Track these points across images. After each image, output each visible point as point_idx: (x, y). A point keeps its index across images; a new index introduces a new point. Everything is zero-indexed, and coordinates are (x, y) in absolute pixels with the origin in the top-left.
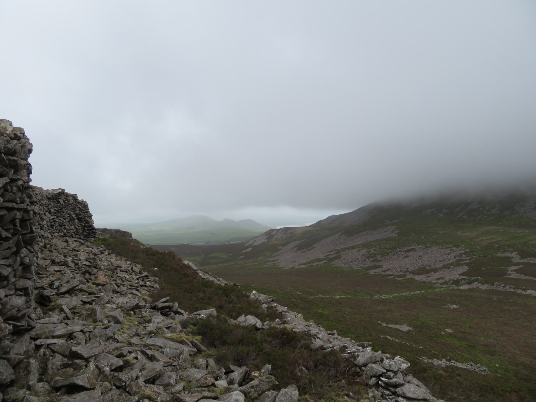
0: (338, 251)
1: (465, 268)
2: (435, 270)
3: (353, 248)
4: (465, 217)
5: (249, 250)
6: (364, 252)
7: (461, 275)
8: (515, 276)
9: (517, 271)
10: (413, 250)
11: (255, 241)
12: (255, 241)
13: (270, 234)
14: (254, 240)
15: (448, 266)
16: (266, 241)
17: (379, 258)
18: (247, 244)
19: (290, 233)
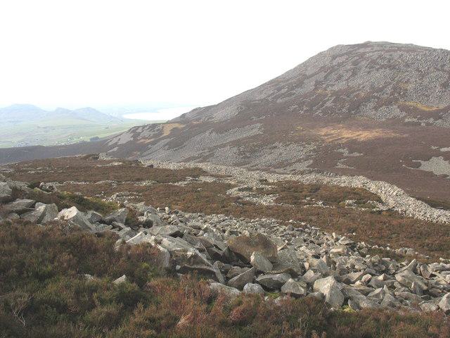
0: (211, 150)
1: (312, 161)
2: (290, 164)
3: (224, 146)
4: (321, 115)
5: (115, 149)
6: (235, 149)
7: (308, 167)
8: (340, 166)
9: (343, 163)
10: (275, 147)
11: (119, 139)
12: (119, 139)
13: (135, 131)
14: (119, 137)
15: (299, 161)
16: (132, 139)
17: (248, 155)
18: (110, 144)
19: (158, 130)
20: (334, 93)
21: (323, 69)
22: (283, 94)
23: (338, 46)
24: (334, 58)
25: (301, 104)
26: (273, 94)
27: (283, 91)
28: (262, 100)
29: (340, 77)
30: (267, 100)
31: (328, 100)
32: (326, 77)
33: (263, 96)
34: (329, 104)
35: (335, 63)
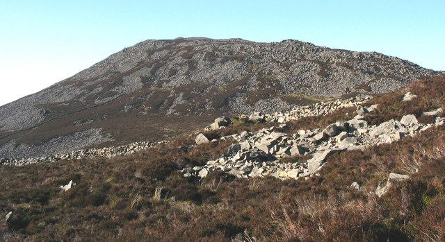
20: (178, 90)
21: (141, 64)
22: (100, 93)
23: (148, 41)
24: (151, 52)
25: (137, 104)
26: (83, 94)
27: (96, 90)
28: (71, 102)
29: (173, 72)
30: (79, 102)
31: (174, 98)
32: (153, 73)
33: (66, 97)
34: (180, 100)
35: (156, 56)
